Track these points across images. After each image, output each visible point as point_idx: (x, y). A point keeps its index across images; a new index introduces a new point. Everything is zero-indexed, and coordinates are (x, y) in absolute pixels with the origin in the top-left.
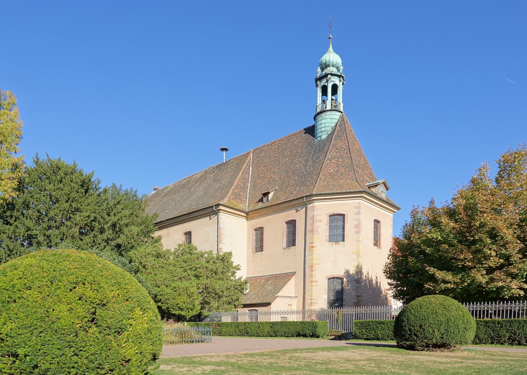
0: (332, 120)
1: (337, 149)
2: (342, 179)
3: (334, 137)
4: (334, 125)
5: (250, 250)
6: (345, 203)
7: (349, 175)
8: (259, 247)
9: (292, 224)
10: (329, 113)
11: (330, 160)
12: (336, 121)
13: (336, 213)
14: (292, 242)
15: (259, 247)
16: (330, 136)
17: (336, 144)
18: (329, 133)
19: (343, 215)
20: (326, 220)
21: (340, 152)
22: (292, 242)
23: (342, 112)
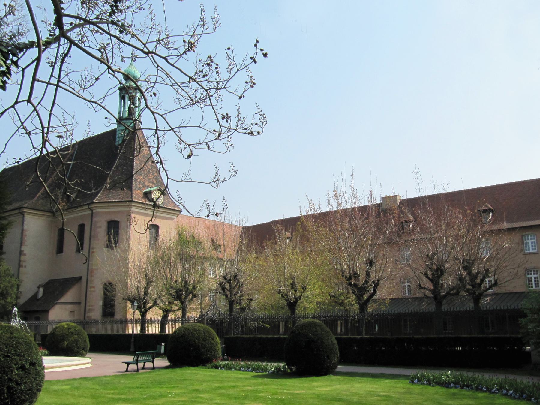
5: (55, 251)
13: (113, 220)
19: (118, 222)
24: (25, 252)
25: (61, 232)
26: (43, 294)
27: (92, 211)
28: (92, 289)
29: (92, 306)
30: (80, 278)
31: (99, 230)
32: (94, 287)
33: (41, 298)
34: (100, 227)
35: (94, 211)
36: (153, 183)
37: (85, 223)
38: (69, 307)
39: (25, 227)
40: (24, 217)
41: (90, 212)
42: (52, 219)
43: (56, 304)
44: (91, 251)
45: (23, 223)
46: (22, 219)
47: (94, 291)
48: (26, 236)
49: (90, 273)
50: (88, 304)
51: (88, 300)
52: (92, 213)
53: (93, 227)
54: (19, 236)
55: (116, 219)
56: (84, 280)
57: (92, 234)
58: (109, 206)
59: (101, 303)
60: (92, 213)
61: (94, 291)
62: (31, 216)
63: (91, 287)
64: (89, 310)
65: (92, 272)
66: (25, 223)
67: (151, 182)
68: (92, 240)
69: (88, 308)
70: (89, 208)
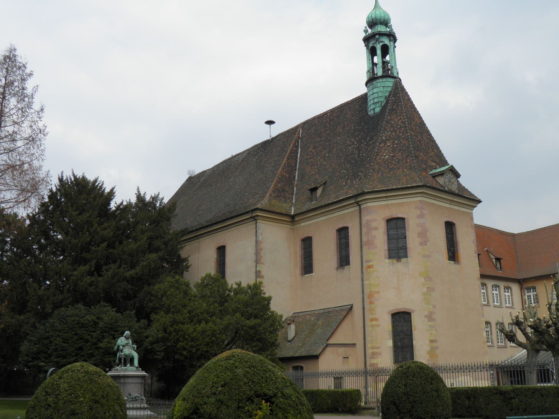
0: (386, 89)
1: (392, 126)
2: (399, 168)
3: (387, 110)
4: (387, 94)
5: (298, 271)
6: (403, 203)
7: (407, 162)
8: (307, 267)
9: (343, 233)
10: (381, 80)
11: (385, 142)
12: (389, 89)
13: (394, 216)
14: (344, 260)
15: (307, 267)
16: (384, 108)
17: (391, 120)
18: (383, 104)
19: (403, 219)
20: (382, 227)
21: (395, 131)
22: (344, 260)
23: (395, 78)
24: (262, 274)
25: (307, 243)
26: (296, 333)
27: (360, 205)
28: (374, 323)
29: (379, 348)
30: (351, 308)
31: (374, 233)
32: (376, 320)
33: (293, 338)
34: (376, 229)
35: (362, 207)
36: (435, 162)
37: (350, 225)
38: (341, 350)
39: (260, 238)
40: (256, 223)
41: (357, 208)
42: (289, 226)
43: (327, 345)
44: (365, 265)
45: (256, 231)
46: (254, 226)
47: (378, 326)
48: (261, 250)
49: (367, 298)
50: (369, 345)
51: (368, 339)
52: (360, 209)
53: (364, 230)
54: (251, 251)
55: (400, 216)
56: (358, 310)
57: (364, 239)
58: (387, 197)
59: (390, 343)
60: (360, 209)
61: (378, 326)
62: (266, 222)
63: (372, 320)
64: (373, 354)
65: (371, 296)
66: (259, 231)
67: (433, 161)
68: (364, 249)
69: (369, 351)
70: (357, 203)
